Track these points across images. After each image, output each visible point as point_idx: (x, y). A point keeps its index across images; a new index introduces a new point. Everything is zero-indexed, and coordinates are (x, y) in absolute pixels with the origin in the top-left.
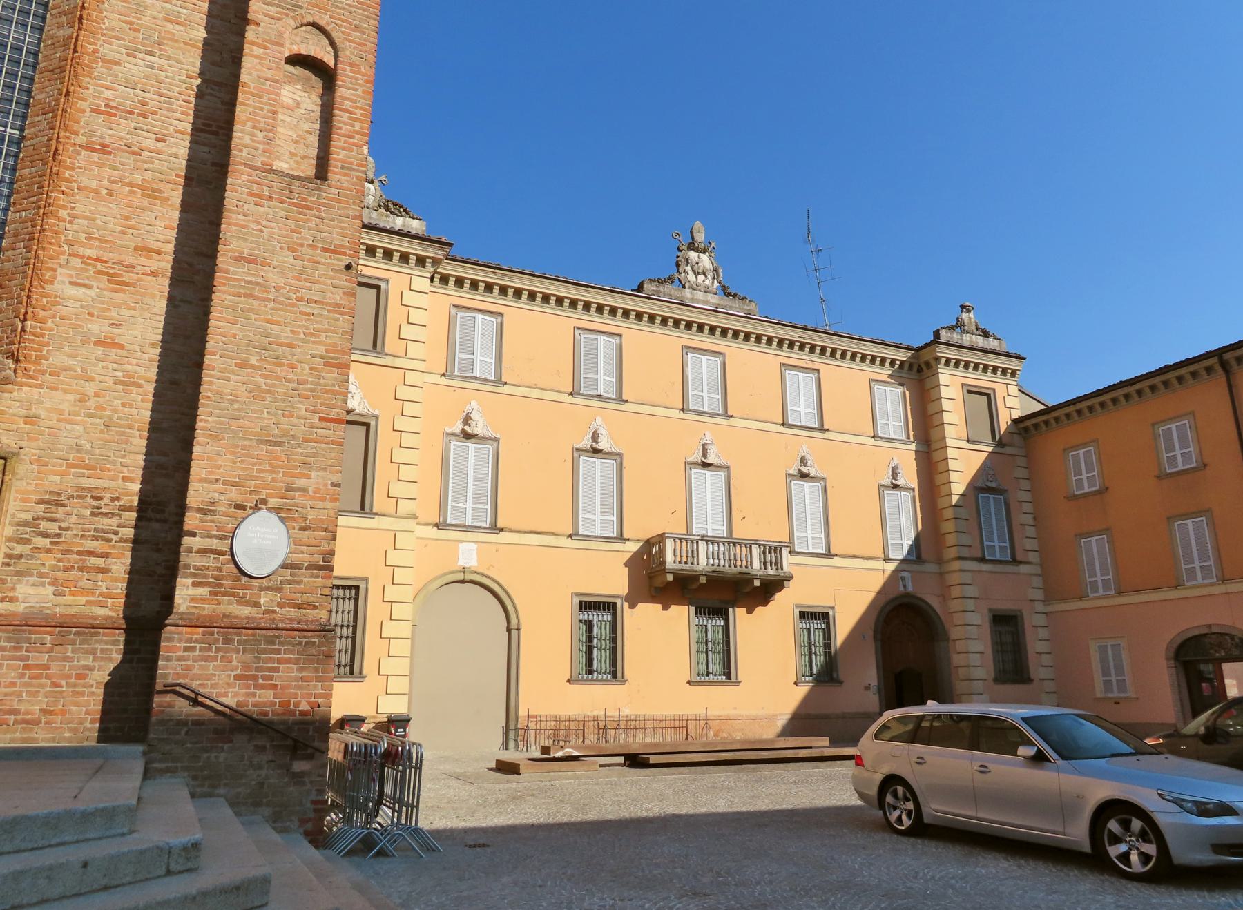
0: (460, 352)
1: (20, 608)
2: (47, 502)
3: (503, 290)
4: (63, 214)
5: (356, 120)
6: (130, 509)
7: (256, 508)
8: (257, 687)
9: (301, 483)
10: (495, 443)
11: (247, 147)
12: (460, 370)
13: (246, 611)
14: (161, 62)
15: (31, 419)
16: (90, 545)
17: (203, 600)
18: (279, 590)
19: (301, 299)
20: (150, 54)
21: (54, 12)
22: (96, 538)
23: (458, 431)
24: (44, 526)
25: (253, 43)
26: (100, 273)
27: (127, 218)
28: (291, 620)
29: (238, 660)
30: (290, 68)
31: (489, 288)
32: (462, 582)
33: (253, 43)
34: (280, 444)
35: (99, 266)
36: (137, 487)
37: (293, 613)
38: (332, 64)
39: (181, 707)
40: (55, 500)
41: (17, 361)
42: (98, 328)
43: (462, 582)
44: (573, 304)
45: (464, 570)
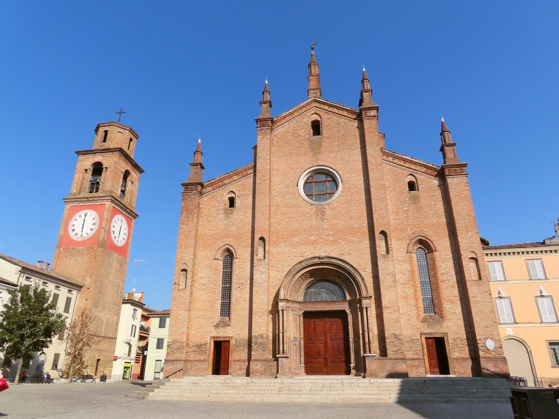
0: (492, 274)
1: (455, 356)
2: (454, 340)
3: (500, 254)
4: (442, 293)
5: (483, 267)
6: (466, 340)
7: (487, 339)
8: (497, 368)
9: (493, 333)
10: (509, 298)
11: (468, 277)
12: (493, 279)
13: (491, 356)
14: (448, 263)
15: (448, 327)
16: (462, 346)
17: (484, 354)
18: (495, 352)
19: (484, 302)
20: (445, 262)
21: (428, 258)
22: (462, 345)
23: (497, 297)
24: (455, 344)
25: (463, 259)
26: (450, 302)
27: (451, 292)
28: (499, 357)
29: (492, 364)
30: (469, 260)
31: (496, 254)
32: (510, 339)
33: (463, 259)
34: (488, 327)
35: (449, 301)
36: (465, 336)
37: (498, 355)
38: (476, 257)
39: (486, 371)
40: (455, 340)
41: (443, 318)
42: (452, 311)
43: (510, 339)
44: (523, 253)
45: (509, 336)
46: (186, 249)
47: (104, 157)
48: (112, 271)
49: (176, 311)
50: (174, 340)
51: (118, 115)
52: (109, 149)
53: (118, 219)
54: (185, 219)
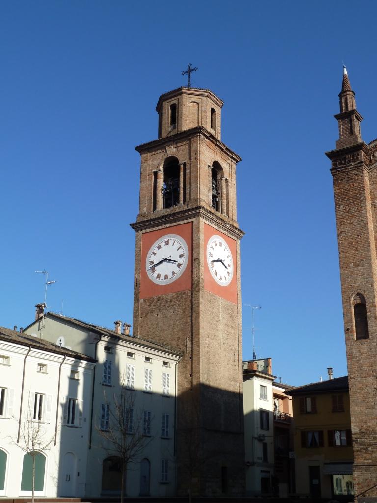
46: (356, 269)
47: (178, 147)
48: (221, 327)
49: (359, 379)
50: (363, 430)
51: (186, 76)
52: (185, 132)
53: (216, 243)
54: (345, 214)
